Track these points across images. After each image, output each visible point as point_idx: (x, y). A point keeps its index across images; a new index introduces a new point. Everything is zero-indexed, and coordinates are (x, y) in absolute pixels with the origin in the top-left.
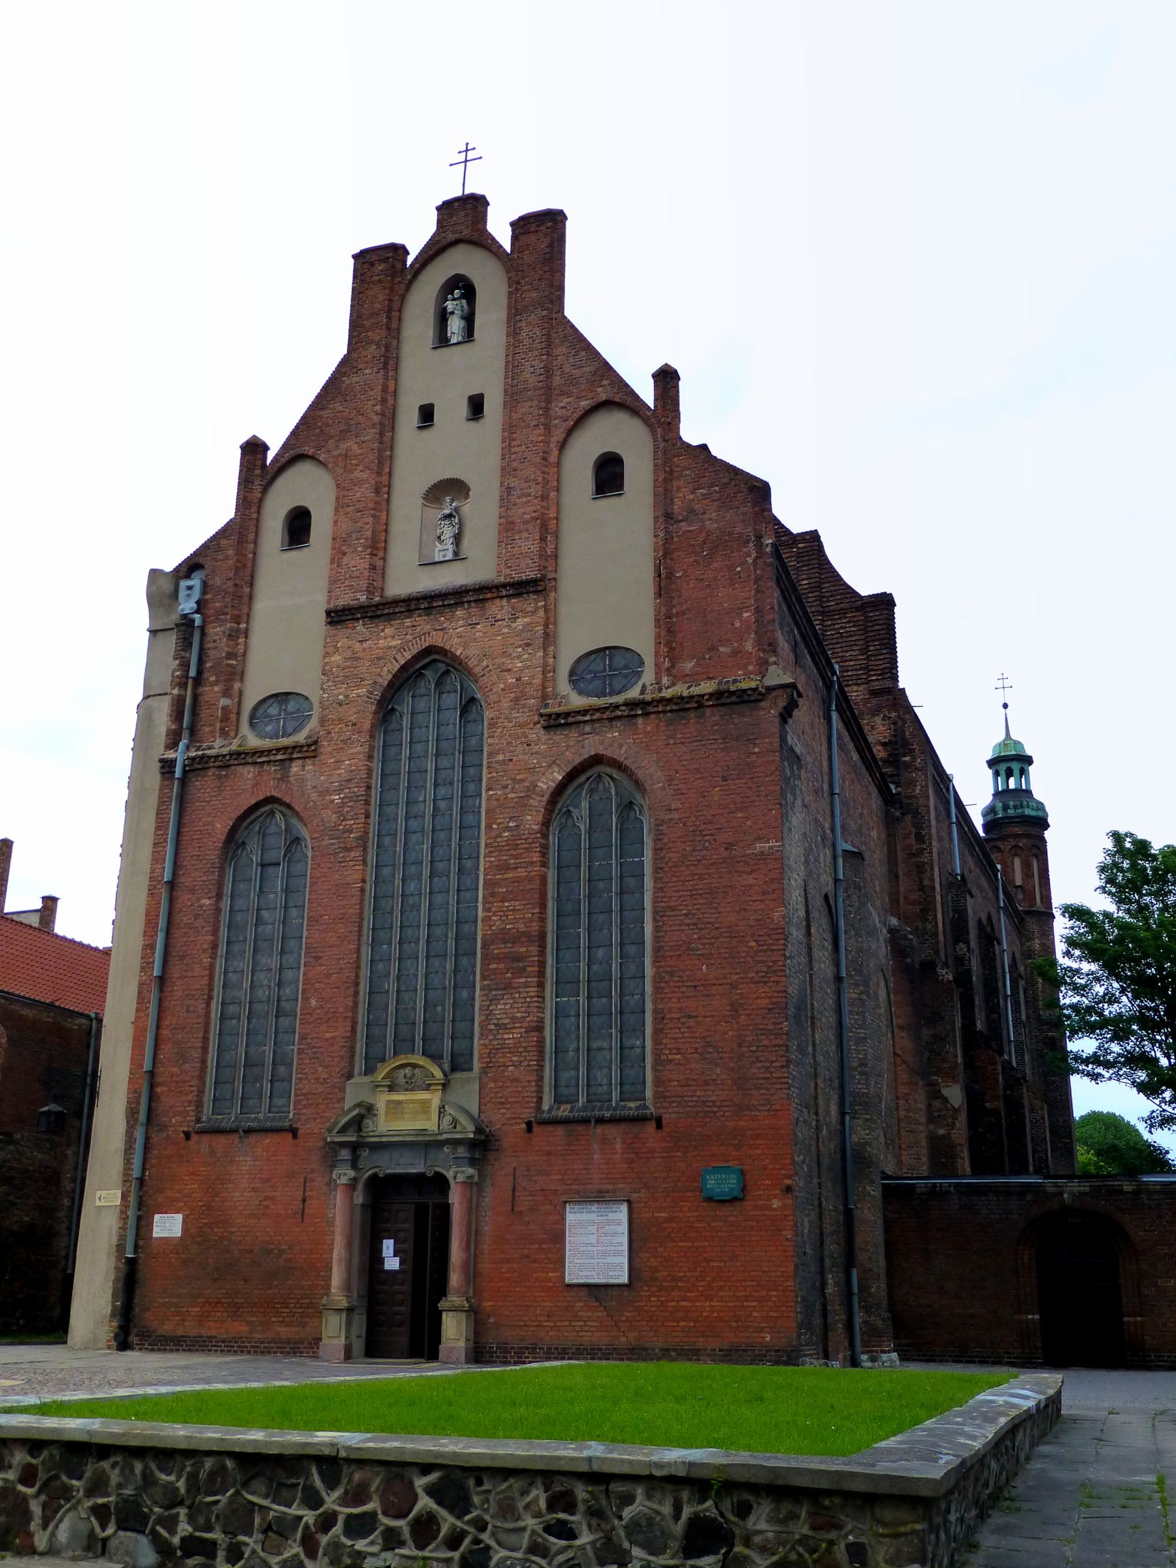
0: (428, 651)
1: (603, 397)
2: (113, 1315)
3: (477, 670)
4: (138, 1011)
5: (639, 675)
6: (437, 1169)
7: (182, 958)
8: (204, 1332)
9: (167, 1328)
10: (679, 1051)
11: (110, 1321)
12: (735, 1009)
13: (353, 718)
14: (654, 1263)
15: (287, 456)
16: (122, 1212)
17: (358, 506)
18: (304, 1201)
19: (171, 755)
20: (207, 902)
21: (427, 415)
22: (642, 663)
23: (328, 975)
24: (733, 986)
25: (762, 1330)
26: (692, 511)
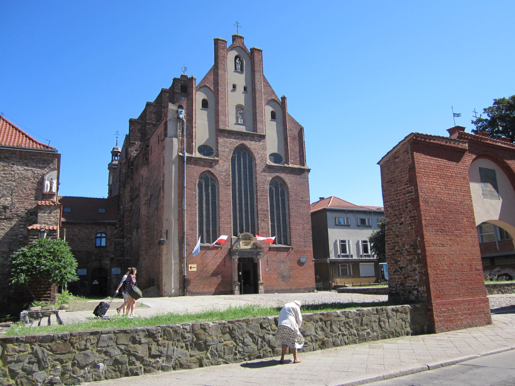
0: (241, 144)
1: (273, 98)
2: (180, 288)
3: (253, 152)
4: (179, 217)
5: (282, 160)
6: (253, 256)
7: (189, 205)
8: (204, 291)
9: (195, 291)
10: (295, 236)
11: (179, 290)
12: (304, 229)
13: (226, 156)
14: (292, 274)
15: (203, 85)
16: (180, 265)
17: (223, 104)
18: (225, 262)
19: (181, 154)
20: (194, 193)
21: (234, 86)
22: (282, 158)
23: (226, 214)
24: (303, 224)
25: (309, 285)
26: (291, 129)
